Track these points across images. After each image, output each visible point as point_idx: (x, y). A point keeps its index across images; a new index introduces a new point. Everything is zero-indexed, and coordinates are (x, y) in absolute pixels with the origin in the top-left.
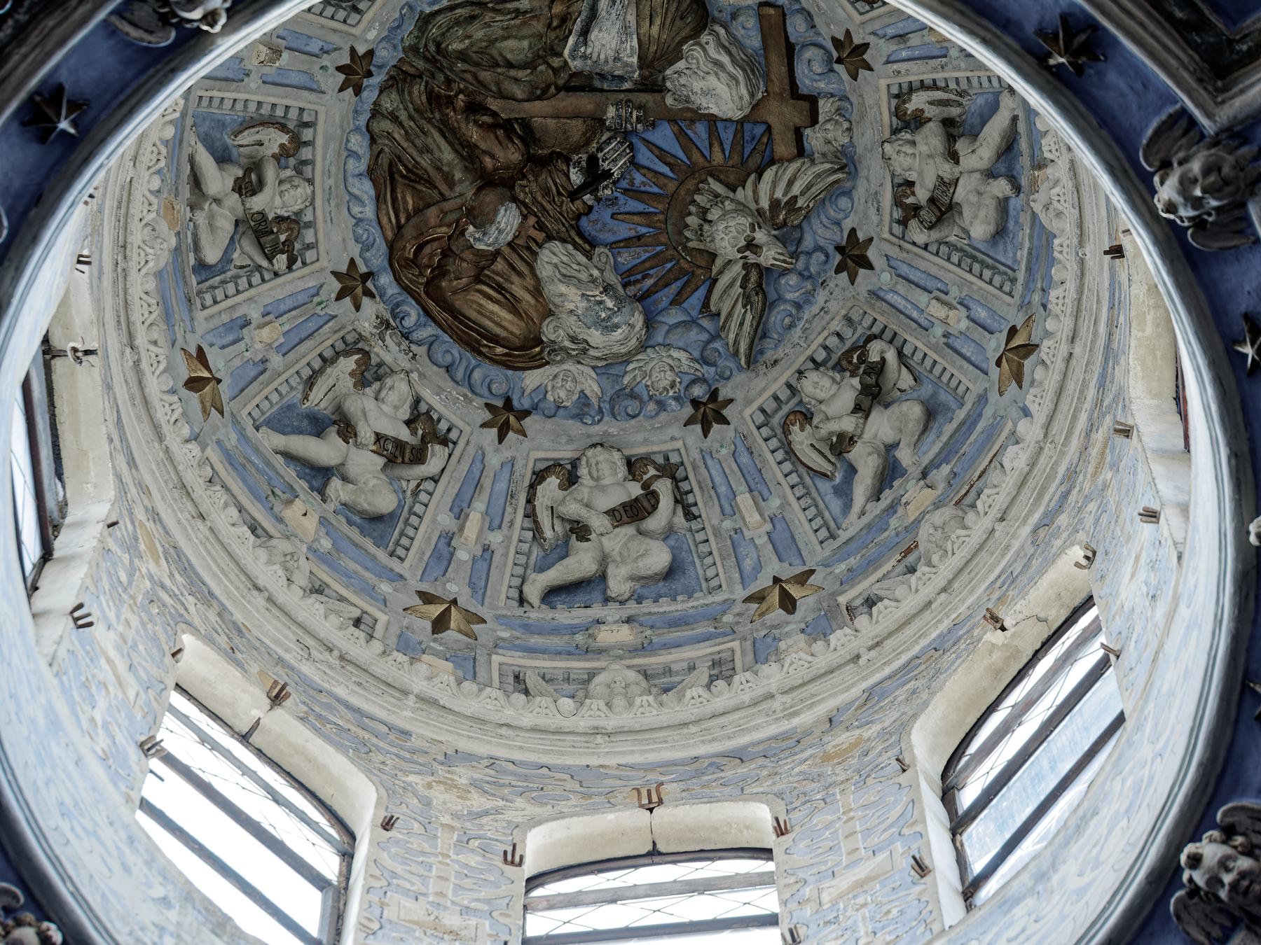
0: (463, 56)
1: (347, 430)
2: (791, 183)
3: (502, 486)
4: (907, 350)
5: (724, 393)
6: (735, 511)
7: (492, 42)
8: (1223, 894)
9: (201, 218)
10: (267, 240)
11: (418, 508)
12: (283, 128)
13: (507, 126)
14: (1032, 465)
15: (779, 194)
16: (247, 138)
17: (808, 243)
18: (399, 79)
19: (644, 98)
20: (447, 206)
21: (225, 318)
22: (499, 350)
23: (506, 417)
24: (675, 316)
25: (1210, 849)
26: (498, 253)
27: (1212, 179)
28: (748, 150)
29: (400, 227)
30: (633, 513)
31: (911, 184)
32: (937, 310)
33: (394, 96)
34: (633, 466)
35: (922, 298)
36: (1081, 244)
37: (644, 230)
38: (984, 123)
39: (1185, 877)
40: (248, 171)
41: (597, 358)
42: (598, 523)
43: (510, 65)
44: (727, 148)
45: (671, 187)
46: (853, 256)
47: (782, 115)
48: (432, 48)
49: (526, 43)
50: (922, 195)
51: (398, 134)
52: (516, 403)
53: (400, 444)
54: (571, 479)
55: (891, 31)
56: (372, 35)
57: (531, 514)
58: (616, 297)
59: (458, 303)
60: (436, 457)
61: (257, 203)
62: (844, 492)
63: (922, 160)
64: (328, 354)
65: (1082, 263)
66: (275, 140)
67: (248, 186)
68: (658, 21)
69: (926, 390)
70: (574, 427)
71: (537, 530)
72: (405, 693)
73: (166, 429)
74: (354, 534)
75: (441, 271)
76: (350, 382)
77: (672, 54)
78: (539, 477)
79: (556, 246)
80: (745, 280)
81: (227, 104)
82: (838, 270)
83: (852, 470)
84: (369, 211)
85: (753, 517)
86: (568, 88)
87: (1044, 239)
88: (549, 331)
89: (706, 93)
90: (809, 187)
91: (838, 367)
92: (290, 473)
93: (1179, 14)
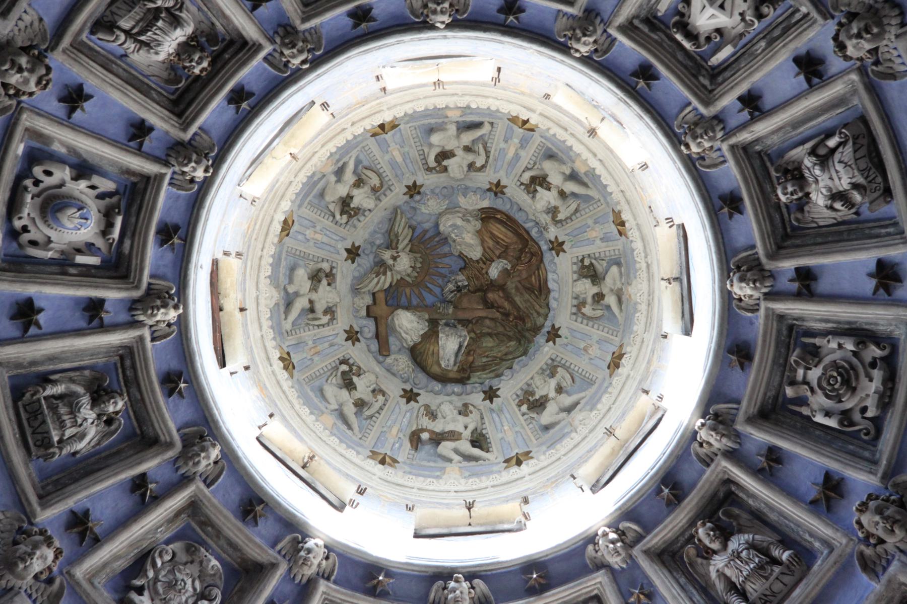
0: (510, 339)
1: (562, 194)
2: (378, 282)
3: (499, 163)
4: (331, 218)
5: (407, 197)
6: (403, 155)
7: (498, 345)
8: (194, 157)
9: (619, 285)
10: (592, 273)
11: (534, 159)
12: (584, 314)
13: (492, 307)
14: (279, 204)
15: (383, 278)
16: (599, 313)
17: (371, 257)
18: (536, 330)
19: (436, 316)
20: (518, 279)
21: (610, 243)
22: (499, 216)
23: (497, 189)
24: (427, 226)
25: (200, 174)
26: (499, 257)
27: (197, 460)
28: (395, 297)
29: (538, 269)
30: (444, 155)
31: (329, 284)
32: (318, 237)
33: (538, 323)
34: (445, 169)
35: (325, 239)
36: (258, 296)
37: (439, 260)
38: (299, 315)
39: (210, 162)
40: (598, 302)
41: (459, 212)
42: (460, 152)
43: (490, 335)
44: (404, 295)
45: (427, 278)
46: (353, 253)
47: (381, 309)
48: (522, 342)
49: (484, 345)
50: (324, 282)
51: (537, 307)
52: (493, 194)
53: (541, 185)
54: (471, 166)
55: (336, 347)
56: (546, 349)
57: (487, 153)
58: (451, 238)
59: (515, 239)
60: (526, 177)
61: (595, 290)
62: (358, 162)
63: (325, 296)
64: (569, 221)
65: (257, 289)
66: (587, 310)
67: (599, 297)
68: (431, 352)
69: (323, 203)
70: (469, 184)
71: (485, 148)
72: (541, 114)
73: (635, 227)
74: (560, 154)
75: (521, 251)
76: (561, 209)
77: (425, 337)
78: (483, 167)
79: (474, 258)
80: (397, 243)
81: (606, 330)
82: (359, 247)
83: (355, 172)
84: (550, 276)
85: (396, 154)
86: (469, 321)
87: (273, 279)
88: (478, 225)
89: (412, 322)
90: (371, 282)
91: (359, 209)
92: (586, 180)
93: (209, 529)
